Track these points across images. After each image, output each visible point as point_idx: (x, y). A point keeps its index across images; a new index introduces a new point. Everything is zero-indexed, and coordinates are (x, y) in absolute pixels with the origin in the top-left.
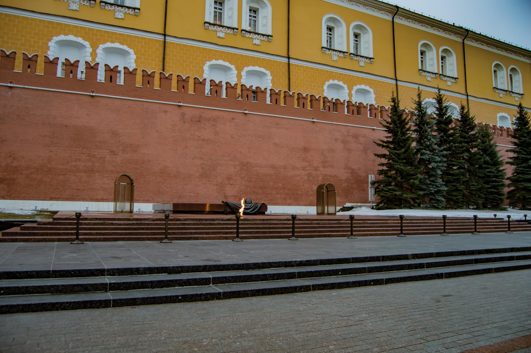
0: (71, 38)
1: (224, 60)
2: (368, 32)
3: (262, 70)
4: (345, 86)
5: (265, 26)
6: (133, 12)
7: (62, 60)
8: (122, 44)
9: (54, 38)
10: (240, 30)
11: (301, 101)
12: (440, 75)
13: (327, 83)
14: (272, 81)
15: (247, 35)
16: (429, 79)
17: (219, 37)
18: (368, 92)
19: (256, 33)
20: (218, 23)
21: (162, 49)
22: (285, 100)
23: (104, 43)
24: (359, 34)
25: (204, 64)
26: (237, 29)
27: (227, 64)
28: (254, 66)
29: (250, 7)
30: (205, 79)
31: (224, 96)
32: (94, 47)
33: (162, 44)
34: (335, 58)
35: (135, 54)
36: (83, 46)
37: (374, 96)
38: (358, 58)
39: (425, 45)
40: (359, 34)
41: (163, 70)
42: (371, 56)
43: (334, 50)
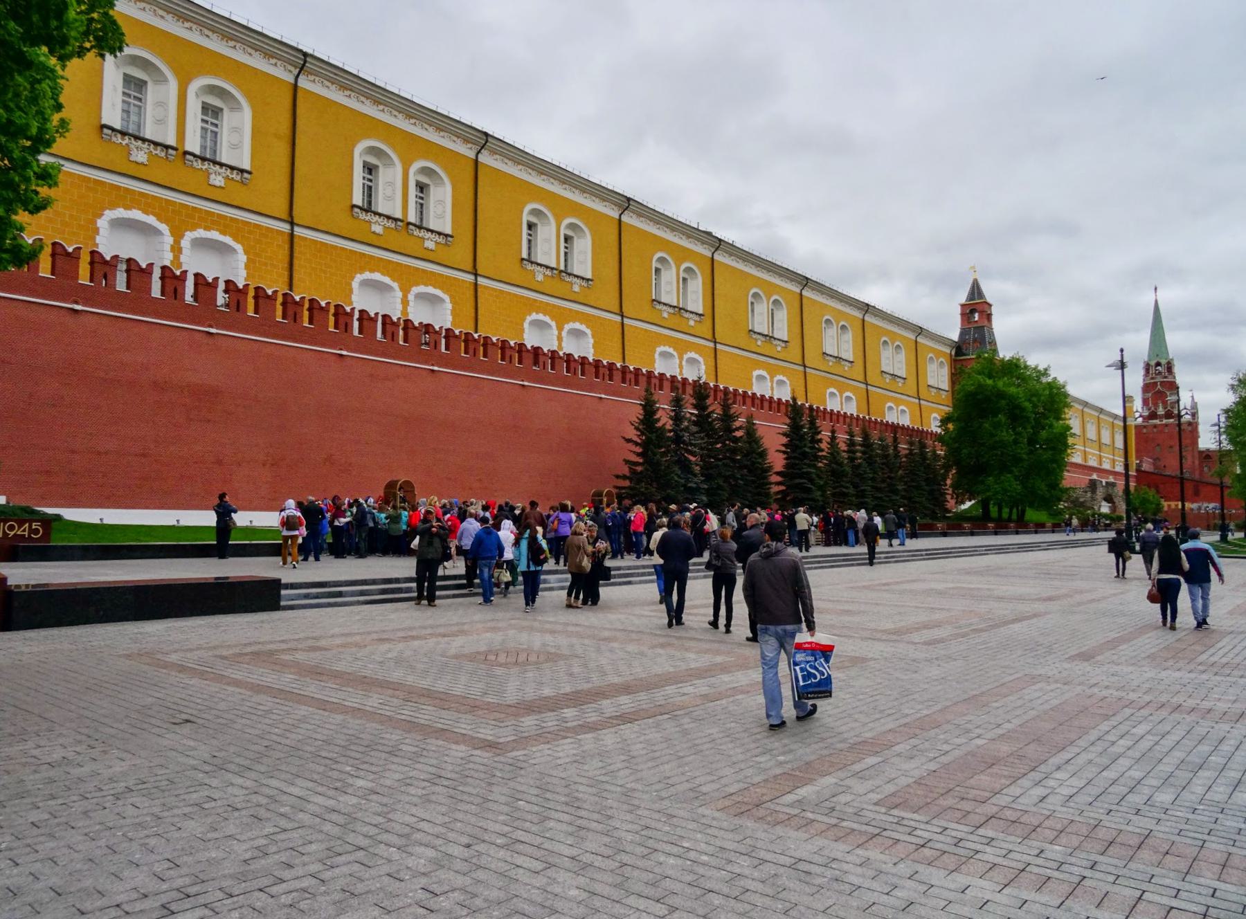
0: (136, 214)
1: (383, 274)
2: (549, 223)
3: (438, 292)
4: (553, 324)
5: (440, 217)
6: (238, 178)
7: (48, 242)
8: (223, 233)
9: (107, 212)
10: (181, 151)
11: (342, 320)
12: (561, 271)
13: (529, 319)
14: (454, 312)
15: (114, 139)
16: (665, 315)
17: (374, 233)
18: (584, 333)
19: (215, 163)
20: (132, 129)
21: (287, 246)
22: (470, 347)
23: (193, 229)
24: (535, 225)
25: (353, 278)
26: (175, 149)
27: (387, 280)
28: (426, 285)
29: (125, 74)
30: (186, 272)
31: (356, 332)
32: (178, 235)
33: (287, 238)
34: (540, 278)
35: (246, 252)
36: (158, 232)
37: (592, 341)
38: (422, 233)
39: (662, 260)
40: (535, 225)
41: (291, 287)
42: (589, 276)
43: (376, 213)
